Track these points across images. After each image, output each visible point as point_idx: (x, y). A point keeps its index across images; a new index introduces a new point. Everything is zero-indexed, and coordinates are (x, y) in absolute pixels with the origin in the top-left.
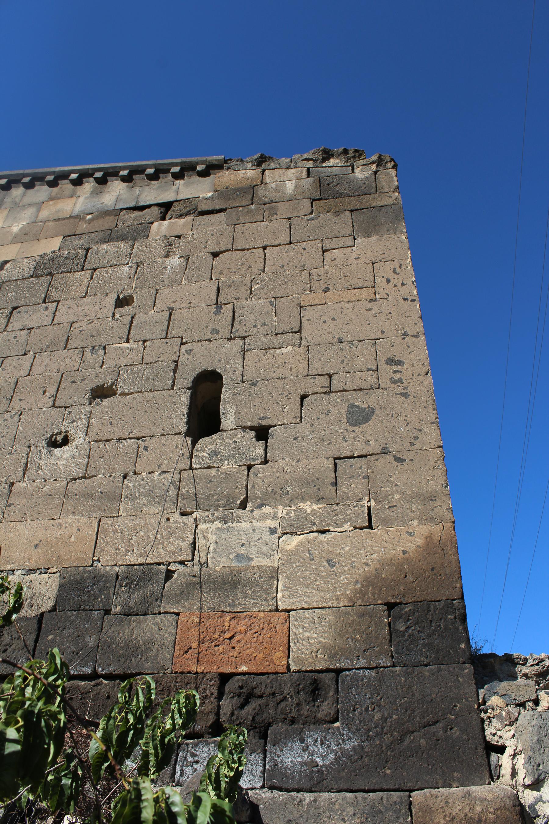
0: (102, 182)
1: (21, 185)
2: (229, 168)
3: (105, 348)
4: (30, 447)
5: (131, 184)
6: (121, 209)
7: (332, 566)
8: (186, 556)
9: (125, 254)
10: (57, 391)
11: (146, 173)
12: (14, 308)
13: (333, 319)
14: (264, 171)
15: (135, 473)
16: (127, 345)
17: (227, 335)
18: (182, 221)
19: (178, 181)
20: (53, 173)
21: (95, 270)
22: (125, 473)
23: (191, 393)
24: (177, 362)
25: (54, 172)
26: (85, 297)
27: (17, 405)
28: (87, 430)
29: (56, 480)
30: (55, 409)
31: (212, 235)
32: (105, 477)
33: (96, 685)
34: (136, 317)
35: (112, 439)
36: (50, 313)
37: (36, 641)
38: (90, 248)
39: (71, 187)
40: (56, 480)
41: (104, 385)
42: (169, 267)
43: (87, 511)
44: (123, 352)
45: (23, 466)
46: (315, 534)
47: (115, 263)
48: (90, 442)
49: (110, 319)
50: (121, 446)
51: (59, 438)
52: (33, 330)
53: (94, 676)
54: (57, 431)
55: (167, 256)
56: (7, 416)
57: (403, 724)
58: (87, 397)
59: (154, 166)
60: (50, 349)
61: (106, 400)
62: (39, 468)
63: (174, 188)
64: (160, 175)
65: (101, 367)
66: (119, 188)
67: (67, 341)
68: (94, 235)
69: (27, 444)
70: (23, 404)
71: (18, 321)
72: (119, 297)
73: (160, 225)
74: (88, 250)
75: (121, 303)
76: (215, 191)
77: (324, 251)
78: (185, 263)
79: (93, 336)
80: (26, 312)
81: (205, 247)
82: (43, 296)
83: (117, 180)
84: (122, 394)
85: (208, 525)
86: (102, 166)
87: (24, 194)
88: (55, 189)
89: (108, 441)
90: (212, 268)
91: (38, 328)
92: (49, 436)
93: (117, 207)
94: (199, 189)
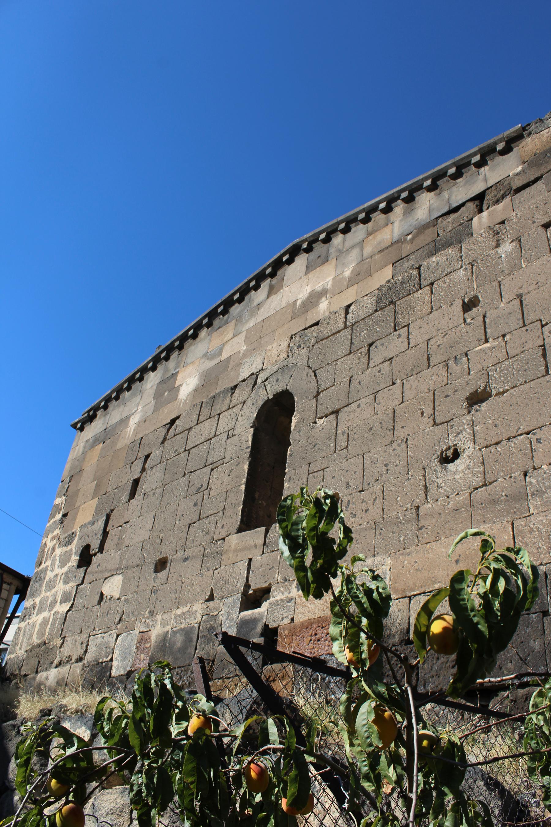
0: (410, 199)
1: (339, 233)
2: (529, 134)
3: (466, 355)
4: (424, 469)
5: (438, 191)
6: (437, 218)
9: (456, 259)
10: (434, 409)
11: (448, 174)
12: (370, 345)
15: (535, 468)
18: (500, 206)
19: (483, 169)
20: (363, 210)
21: (432, 284)
22: (524, 470)
24: (543, 345)
25: (364, 209)
26: (431, 312)
27: (400, 433)
28: (474, 439)
29: (458, 494)
30: (437, 427)
31: (537, 207)
32: (505, 479)
34: (488, 315)
35: (502, 441)
36: (404, 338)
38: (420, 266)
39: (383, 216)
40: (458, 494)
41: (477, 390)
42: (503, 256)
43: (497, 517)
44: (485, 352)
45: (423, 488)
47: (449, 270)
48: (480, 449)
49: (463, 325)
50: (513, 445)
51: (450, 453)
52: (393, 360)
54: (445, 447)
55: (498, 246)
56: (394, 445)
58: (464, 407)
59: (454, 164)
60: (415, 371)
61: (484, 404)
62: (439, 487)
63: (481, 177)
64: (463, 171)
65: (469, 373)
66: (428, 199)
67: (428, 359)
68: (420, 252)
69: (421, 467)
70: (406, 431)
71: (377, 356)
72: (464, 302)
73: (480, 218)
74: (419, 268)
75: (467, 307)
76: (524, 163)
78: (518, 246)
79: (452, 347)
80: (382, 345)
81: (534, 222)
82: (392, 325)
83: (423, 193)
84: (498, 394)
86: (405, 185)
87: (344, 240)
88: (370, 224)
89: (497, 443)
90: (549, 241)
91: (397, 356)
92: (439, 454)
93: (433, 217)
94: (508, 167)
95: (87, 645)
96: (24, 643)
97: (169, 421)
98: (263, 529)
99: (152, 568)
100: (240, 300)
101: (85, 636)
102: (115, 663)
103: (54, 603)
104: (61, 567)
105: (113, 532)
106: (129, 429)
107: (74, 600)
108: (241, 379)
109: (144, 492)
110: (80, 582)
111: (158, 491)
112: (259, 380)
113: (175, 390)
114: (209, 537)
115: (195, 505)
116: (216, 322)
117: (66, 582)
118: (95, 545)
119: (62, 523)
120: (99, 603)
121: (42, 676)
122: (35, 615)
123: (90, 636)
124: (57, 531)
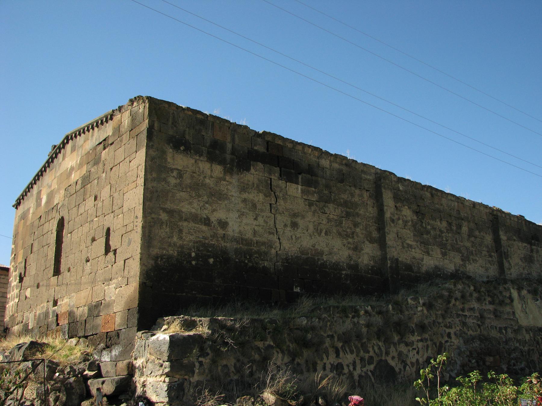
16: (96, 219)
17: (111, 211)
27: (81, 248)
53: (92, 335)
77: (130, 162)
100: (56, 157)
103: (14, 297)
105: (28, 268)
113: (41, 200)
116: (51, 166)
117: (17, 289)
118: (23, 274)
124: (13, 263)
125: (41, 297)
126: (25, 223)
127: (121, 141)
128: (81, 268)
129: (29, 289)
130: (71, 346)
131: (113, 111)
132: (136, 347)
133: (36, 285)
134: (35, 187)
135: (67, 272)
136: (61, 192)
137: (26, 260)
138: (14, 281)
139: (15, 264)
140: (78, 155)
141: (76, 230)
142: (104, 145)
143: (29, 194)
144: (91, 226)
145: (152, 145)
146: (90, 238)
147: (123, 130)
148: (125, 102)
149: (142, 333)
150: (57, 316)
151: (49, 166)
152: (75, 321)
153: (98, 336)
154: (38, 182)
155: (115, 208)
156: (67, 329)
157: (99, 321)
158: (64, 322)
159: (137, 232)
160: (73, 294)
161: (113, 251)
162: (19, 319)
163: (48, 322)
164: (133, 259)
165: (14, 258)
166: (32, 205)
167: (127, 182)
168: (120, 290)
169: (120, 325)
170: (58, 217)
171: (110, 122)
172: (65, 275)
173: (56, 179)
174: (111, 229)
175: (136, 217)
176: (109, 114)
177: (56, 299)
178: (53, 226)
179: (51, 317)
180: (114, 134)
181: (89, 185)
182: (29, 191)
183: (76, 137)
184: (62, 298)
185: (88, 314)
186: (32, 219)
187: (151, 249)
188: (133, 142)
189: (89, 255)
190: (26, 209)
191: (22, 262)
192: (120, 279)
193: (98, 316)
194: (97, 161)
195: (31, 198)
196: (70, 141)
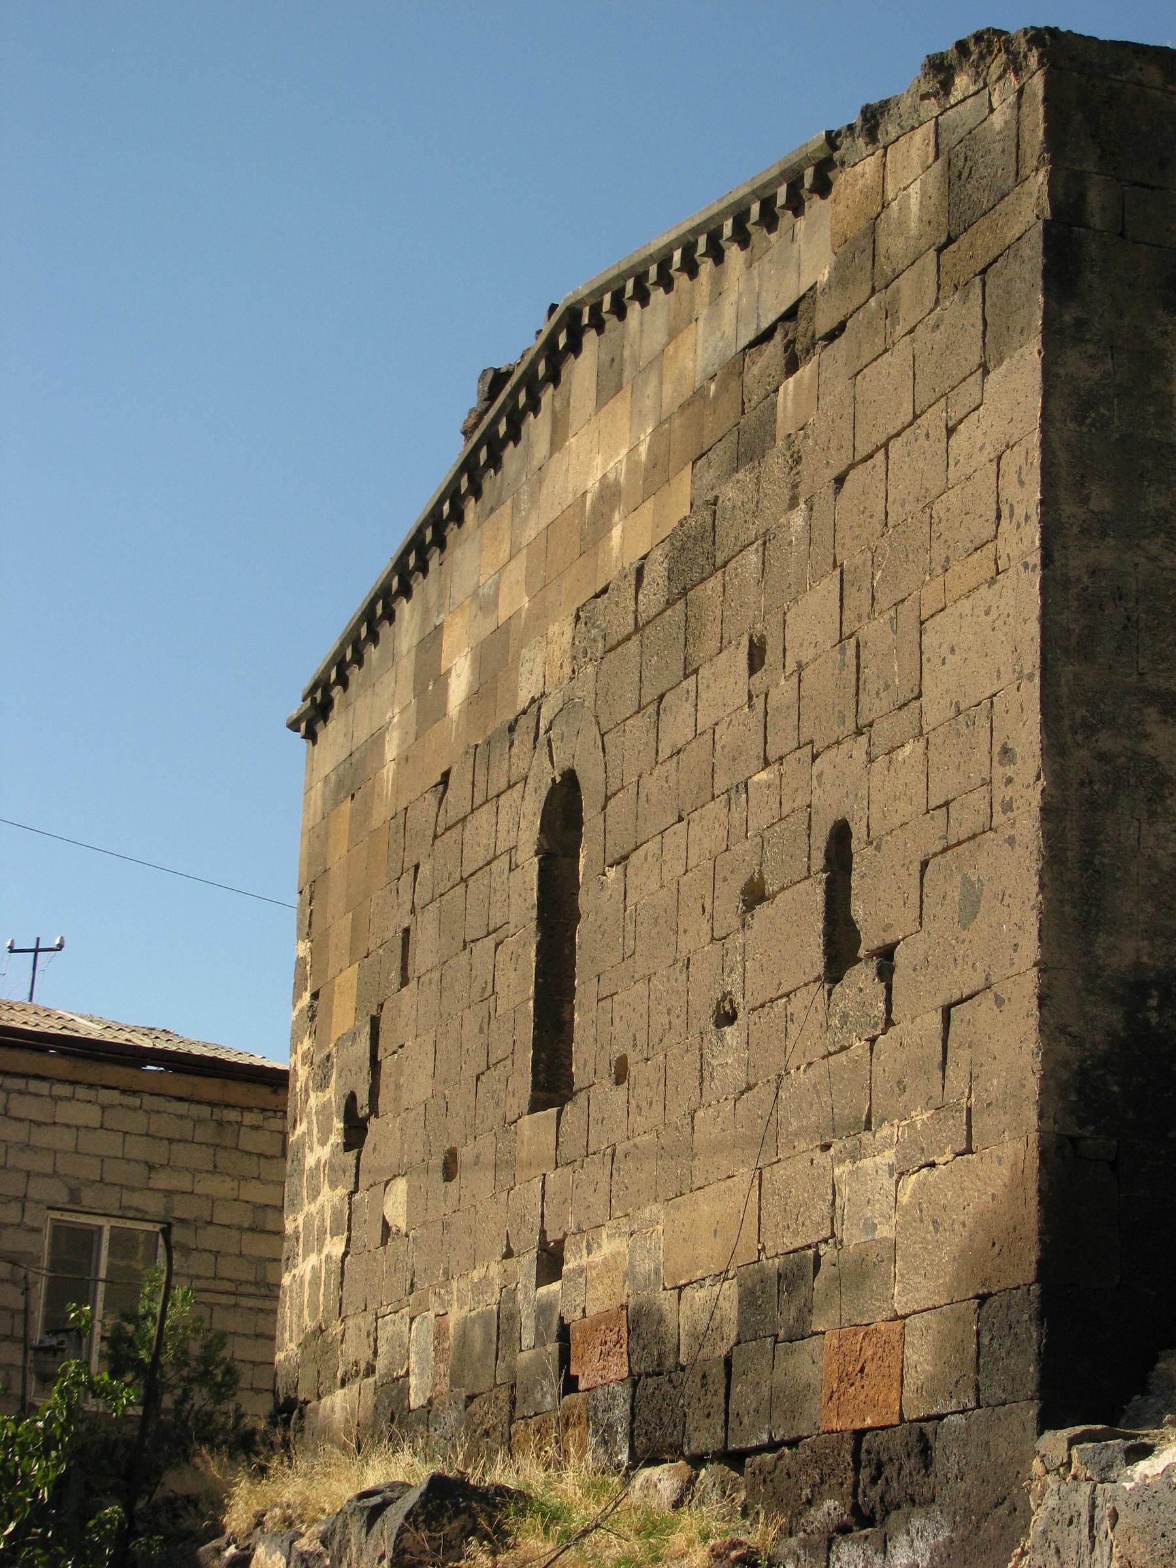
7: (936, 1230)
8: (825, 1233)
13: (952, 651)
14: (885, 148)
16: (763, 776)
17: (851, 726)
23: (829, 882)
24: (809, 806)
27: (686, 943)
33: (780, 1457)
36: (688, 708)
37: (727, 1396)
46: (924, 1170)
53: (772, 1446)
57: (980, 1503)
62: (713, 1078)
72: (751, 641)
77: (950, 431)
85: (842, 1168)
89: (762, 1006)
93: (740, 347)
95: (376, 1340)
96: (294, 1327)
97: (439, 779)
98: (555, 1110)
99: (439, 1176)
100: (514, 435)
101: (371, 1318)
102: (413, 1381)
104: (323, 1142)
105: (387, 1064)
106: (385, 771)
107: (349, 1230)
108: (520, 708)
109: (417, 974)
110: (351, 1188)
111: (435, 975)
112: (543, 724)
114: (500, 1112)
115: (481, 1030)
116: (487, 486)
117: (333, 1186)
118: (363, 1099)
119: (312, 1018)
120: (384, 1242)
121: (326, 1401)
122: (300, 1259)
123: (377, 1319)
124: (307, 1043)
125: (470, 1231)
126: (361, 816)
127: (890, 312)
128: (691, 1058)
129: (400, 1187)
130: (650, 1512)
131: (832, 139)
132: (1035, 1529)
133: (438, 1161)
134: (405, 609)
135: (608, 1082)
136: (554, 629)
137: (375, 1022)
138: (316, 1143)
139: (319, 1046)
140: (636, 415)
141: (652, 846)
142: (789, 345)
143: (372, 653)
144: (737, 815)
145: (1080, 323)
146: (737, 883)
147: (893, 246)
148: (901, 78)
149: (1073, 1441)
150: (564, 1334)
151: (476, 491)
152: (669, 1362)
153: (804, 1452)
154: (418, 585)
155: (874, 705)
156: (621, 1411)
157: (810, 1363)
158: (603, 1369)
159: (1011, 841)
160: (647, 1213)
161: (872, 954)
162: (353, 1351)
163: (512, 1370)
164: (999, 1001)
165: (312, 1013)
166: (395, 715)
167: (939, 551)
168: (922, 1184)
169: (930, 1391)
170: (544, 776)
171: (816, 206)
172: (599, 1101)
173: (522, 557)
174: (858, 831)
175: (1006, 750)
176: (807, 158)
177: (552, 1236)
178: (520, 824)
179: (528, 1339)
180: (841, 278)
181: (714, 584)
182: (373, 637)
183: (620, 310)
184: (589, 1232)
185: (743, 1322)
186: (397, 791)
187: (1103, 940)
188: (964, 313)
189: (733, 983)
190: (362, 735)
191: (354, 1036)
192: (921, 1117)
193: (799, 1334)
194: (750, 443)
195: (389, 677)
196: (590, 340)
